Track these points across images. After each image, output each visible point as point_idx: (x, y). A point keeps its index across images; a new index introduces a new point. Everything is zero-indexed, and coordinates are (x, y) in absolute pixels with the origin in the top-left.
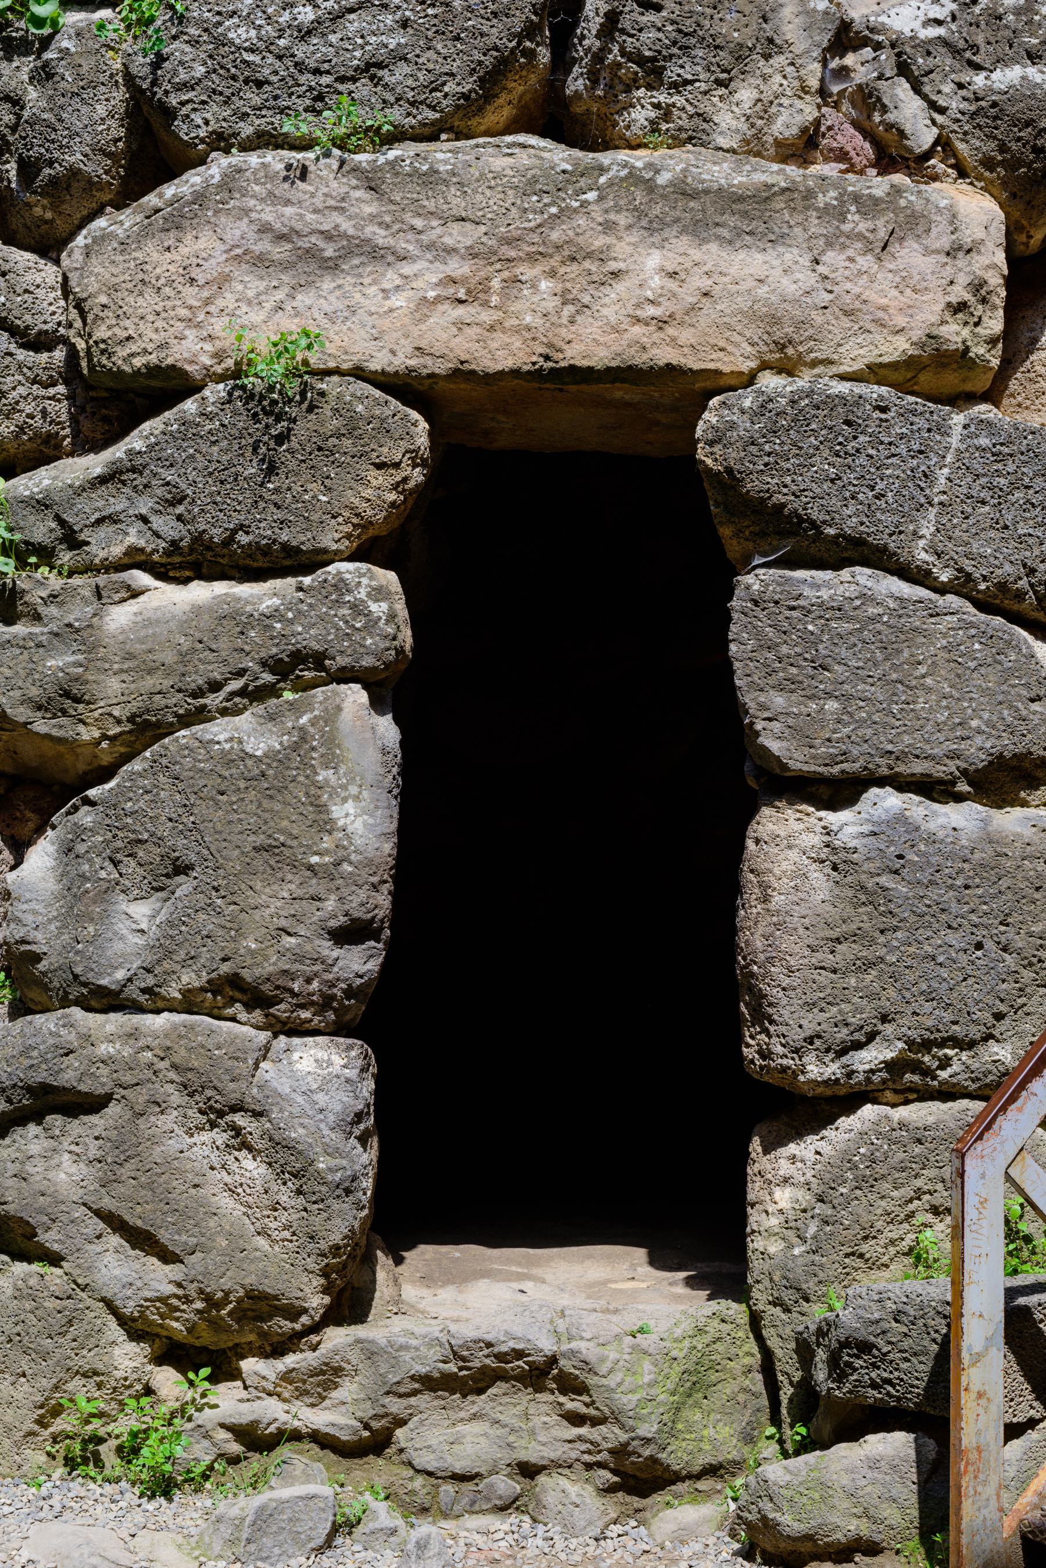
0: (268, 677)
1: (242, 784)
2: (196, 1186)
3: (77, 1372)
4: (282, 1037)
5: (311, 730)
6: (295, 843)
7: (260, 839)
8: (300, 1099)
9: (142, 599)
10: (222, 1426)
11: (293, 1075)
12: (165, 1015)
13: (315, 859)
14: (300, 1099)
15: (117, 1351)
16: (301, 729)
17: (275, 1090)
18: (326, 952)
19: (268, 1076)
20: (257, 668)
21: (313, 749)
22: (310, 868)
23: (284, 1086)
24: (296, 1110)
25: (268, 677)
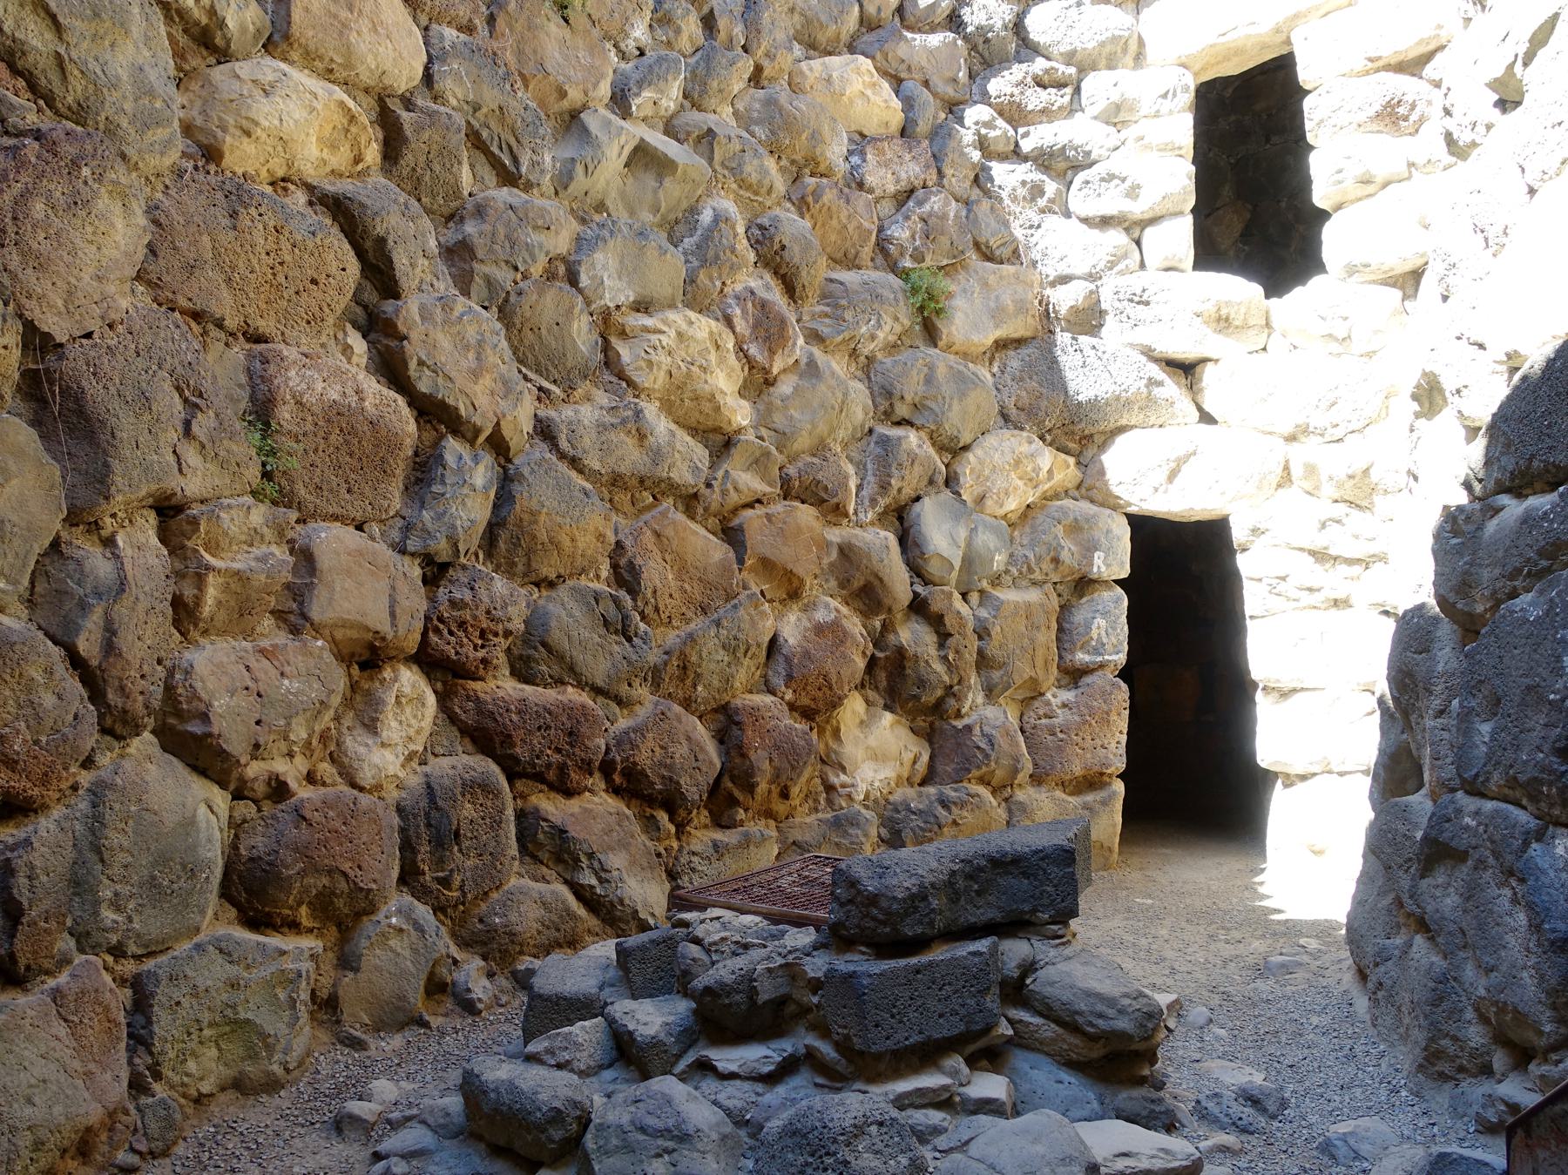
0: (1544, 563)
1: (1524, 641)
2: (1498, 924)
3: (1447, 1035)
4: (1551, 828)
5: (1557, 600)
6: (1543, 684)
7: (1528, 681)
8: (1552, 874)
9: (1502, 514)
10: (1503, 1100)
11: (1553, 857)
12: (1494, 802)
13: (1552, 697)
14: (1552, 874)
15: (1472, 1029)
16: (1551, 600)
17: (1536, 864)
18: (1556, 766)
19: (1534, 854)
20: (1536, 557)
21: (1557, 614)
22: (1550, 702)
23: (1543, 863)
24: (1547, 881)
25: (1544, 563)
